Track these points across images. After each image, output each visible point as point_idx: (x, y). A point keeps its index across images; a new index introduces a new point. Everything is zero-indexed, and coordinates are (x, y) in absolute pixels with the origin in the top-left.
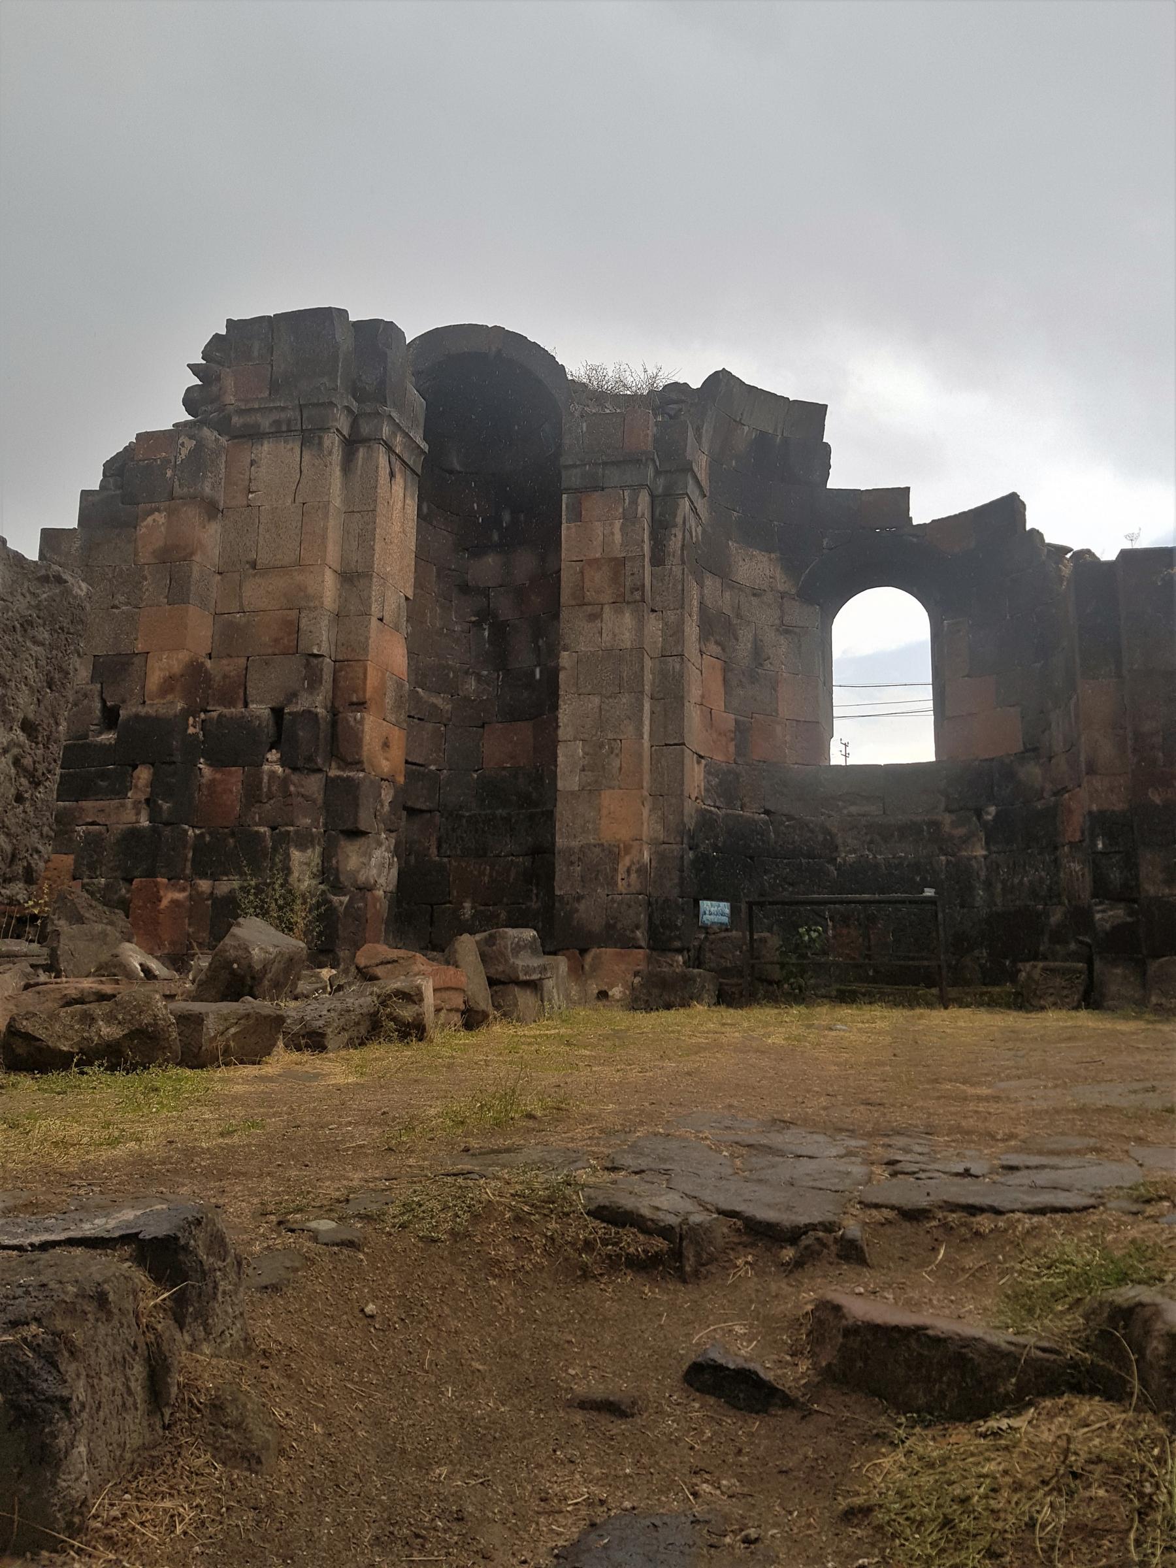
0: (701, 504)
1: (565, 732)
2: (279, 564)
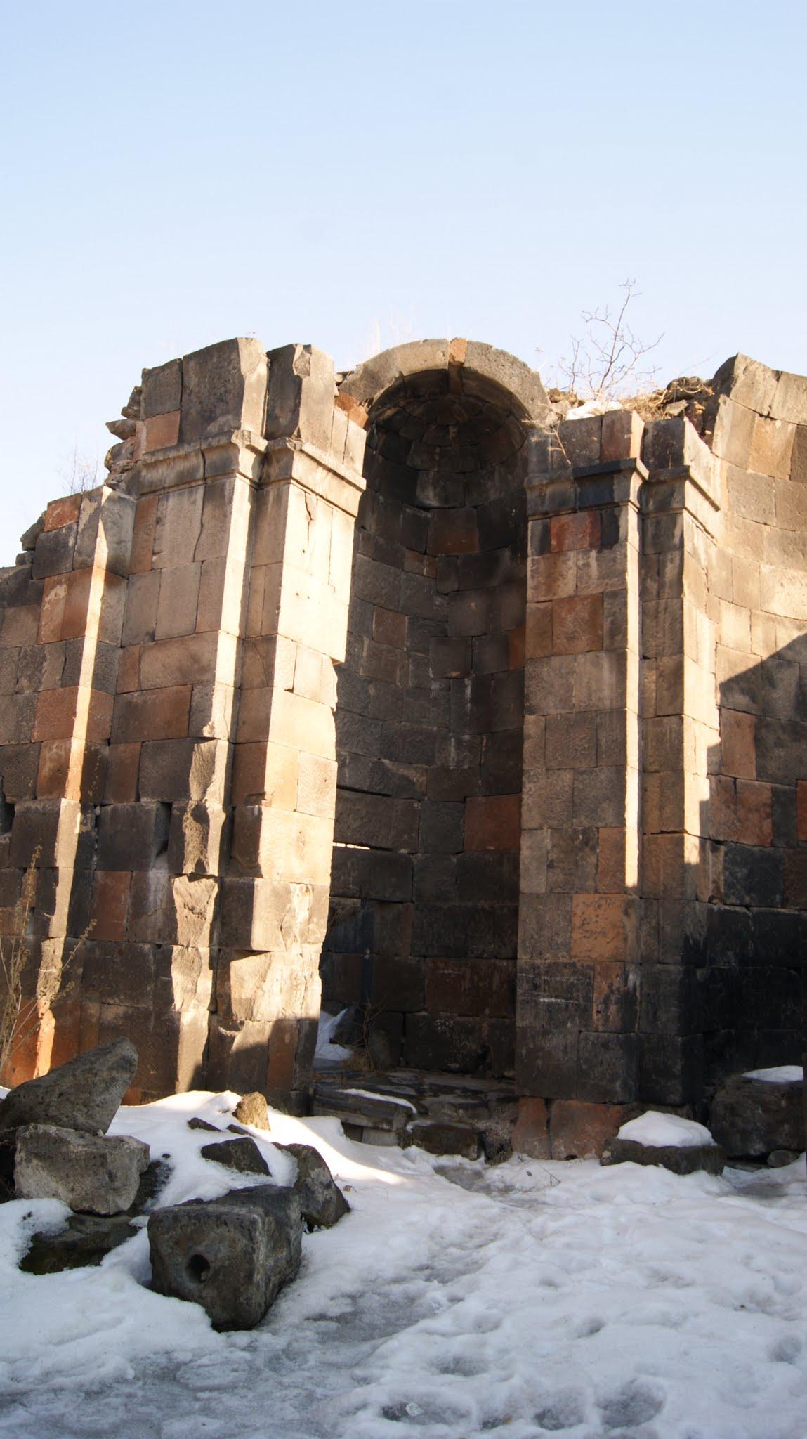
0: (713, 520)
1: (530, 817)
2: (175, 633)
